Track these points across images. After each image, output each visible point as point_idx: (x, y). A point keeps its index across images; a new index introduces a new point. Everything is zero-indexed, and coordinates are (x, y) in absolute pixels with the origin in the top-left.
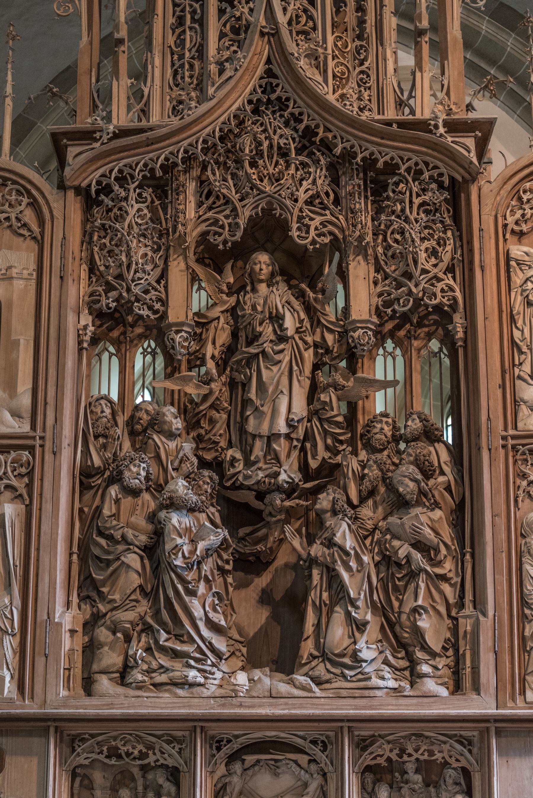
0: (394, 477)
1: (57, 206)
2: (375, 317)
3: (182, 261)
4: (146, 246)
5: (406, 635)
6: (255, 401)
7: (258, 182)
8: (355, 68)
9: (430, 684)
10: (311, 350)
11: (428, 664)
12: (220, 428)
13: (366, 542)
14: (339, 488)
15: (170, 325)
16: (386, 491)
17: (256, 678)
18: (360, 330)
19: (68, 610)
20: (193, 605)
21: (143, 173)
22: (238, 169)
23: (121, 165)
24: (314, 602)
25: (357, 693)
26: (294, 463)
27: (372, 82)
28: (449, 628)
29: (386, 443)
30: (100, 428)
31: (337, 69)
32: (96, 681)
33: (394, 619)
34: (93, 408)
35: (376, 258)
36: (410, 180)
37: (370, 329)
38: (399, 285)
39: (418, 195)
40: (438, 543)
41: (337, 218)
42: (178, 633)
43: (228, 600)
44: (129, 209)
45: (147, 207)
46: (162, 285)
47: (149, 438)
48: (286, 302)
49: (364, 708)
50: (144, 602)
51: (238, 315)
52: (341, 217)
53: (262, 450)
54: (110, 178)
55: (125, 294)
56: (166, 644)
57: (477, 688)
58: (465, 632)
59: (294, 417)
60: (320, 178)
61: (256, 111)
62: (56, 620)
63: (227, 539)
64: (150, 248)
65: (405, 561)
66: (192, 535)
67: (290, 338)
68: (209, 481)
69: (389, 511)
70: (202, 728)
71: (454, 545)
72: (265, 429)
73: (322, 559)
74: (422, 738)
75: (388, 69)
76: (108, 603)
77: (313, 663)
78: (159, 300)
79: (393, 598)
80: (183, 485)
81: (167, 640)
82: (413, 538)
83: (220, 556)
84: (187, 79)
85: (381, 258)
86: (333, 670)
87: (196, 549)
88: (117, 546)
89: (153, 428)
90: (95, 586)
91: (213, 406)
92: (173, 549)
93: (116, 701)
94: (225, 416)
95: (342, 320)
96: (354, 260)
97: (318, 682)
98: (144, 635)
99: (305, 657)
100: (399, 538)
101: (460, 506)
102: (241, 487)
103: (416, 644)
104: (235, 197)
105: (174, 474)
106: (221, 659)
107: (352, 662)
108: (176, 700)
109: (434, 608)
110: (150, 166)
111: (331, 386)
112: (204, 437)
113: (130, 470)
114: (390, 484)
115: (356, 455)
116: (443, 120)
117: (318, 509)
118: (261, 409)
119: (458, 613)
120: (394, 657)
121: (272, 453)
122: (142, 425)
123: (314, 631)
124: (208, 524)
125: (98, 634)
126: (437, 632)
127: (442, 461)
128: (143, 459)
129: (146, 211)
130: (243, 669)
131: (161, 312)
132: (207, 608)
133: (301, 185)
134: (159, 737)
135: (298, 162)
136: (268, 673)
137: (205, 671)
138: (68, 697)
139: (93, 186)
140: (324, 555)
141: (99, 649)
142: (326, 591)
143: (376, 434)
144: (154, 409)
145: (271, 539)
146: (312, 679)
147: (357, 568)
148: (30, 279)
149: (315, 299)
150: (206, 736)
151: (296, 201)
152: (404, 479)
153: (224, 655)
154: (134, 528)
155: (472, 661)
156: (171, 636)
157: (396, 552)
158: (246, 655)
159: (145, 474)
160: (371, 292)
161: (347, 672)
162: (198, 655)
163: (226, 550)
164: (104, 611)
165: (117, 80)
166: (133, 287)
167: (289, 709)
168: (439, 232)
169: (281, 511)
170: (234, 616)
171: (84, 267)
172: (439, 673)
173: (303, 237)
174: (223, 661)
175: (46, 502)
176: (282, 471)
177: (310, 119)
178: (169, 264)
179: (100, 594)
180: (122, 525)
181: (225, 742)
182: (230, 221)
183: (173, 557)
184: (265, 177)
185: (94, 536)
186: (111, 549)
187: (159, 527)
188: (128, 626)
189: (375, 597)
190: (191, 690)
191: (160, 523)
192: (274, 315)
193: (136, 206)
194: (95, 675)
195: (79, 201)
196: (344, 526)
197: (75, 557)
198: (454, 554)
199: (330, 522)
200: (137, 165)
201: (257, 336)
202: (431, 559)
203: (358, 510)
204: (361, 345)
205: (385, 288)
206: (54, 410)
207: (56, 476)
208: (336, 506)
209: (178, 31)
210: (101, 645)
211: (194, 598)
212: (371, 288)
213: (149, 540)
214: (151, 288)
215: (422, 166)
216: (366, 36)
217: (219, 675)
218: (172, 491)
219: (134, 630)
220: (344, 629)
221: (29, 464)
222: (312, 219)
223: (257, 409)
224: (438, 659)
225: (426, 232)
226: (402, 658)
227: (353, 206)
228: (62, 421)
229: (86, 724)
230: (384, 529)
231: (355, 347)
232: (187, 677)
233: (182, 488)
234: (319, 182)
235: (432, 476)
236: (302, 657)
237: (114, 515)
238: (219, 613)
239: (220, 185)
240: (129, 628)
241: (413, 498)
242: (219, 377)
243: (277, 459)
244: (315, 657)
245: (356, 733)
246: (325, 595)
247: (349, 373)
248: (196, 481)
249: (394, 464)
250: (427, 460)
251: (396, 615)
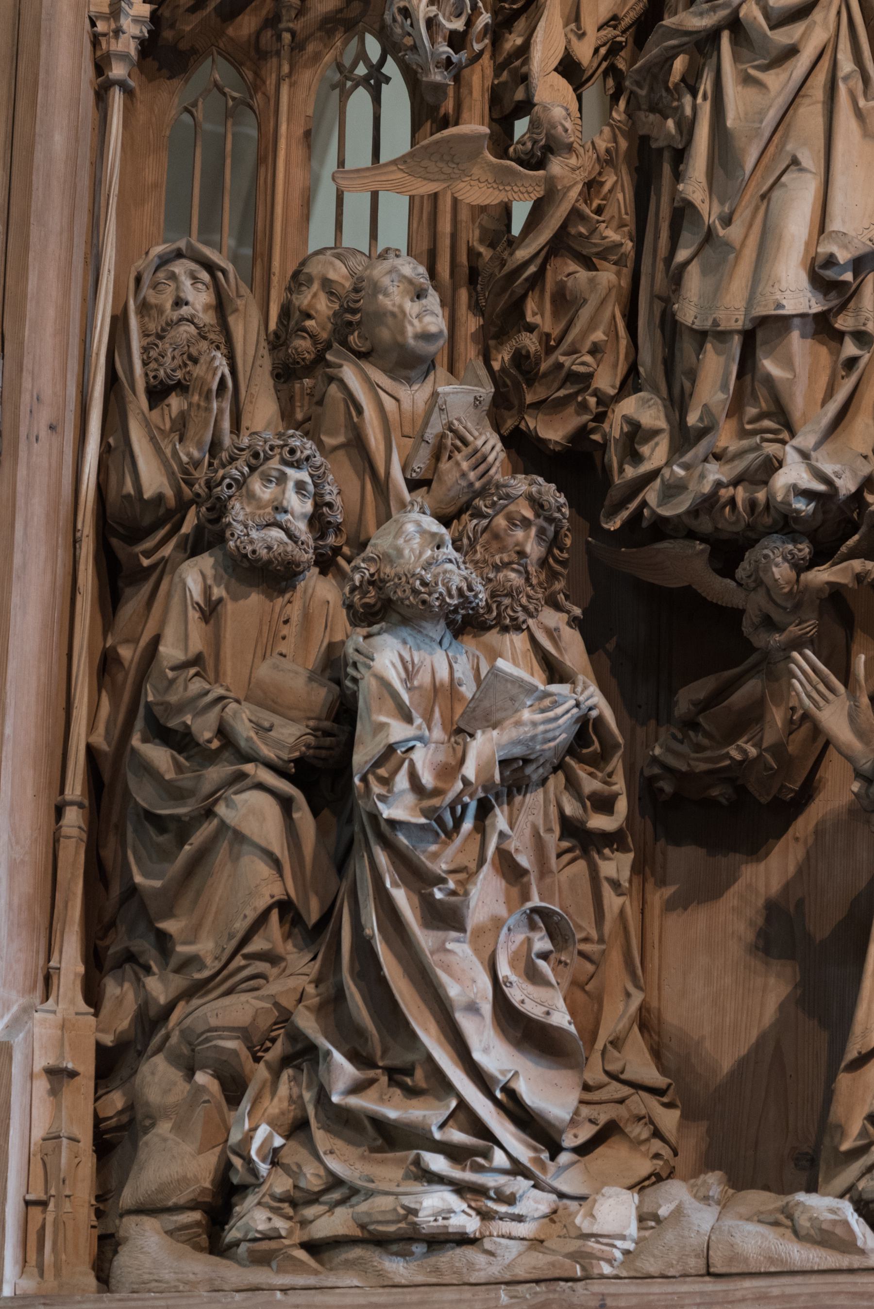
20: (451, 958)
42: (397, 1062)
56: (354, 1101)
68: (529, 514)
80: (423, 532)
81: (357, 1088)
89: (344, 343)
92: (379, 763)
98: (287, 1073)
106: (555, 1150)
113: (251, 496)
128: (292, 452)
132: (504, 970)
156: (371, 1074)
174: (564, 1158)
176: (791, 456)
211: (453, 934)
218: (385, 558)
233: (416, 541)
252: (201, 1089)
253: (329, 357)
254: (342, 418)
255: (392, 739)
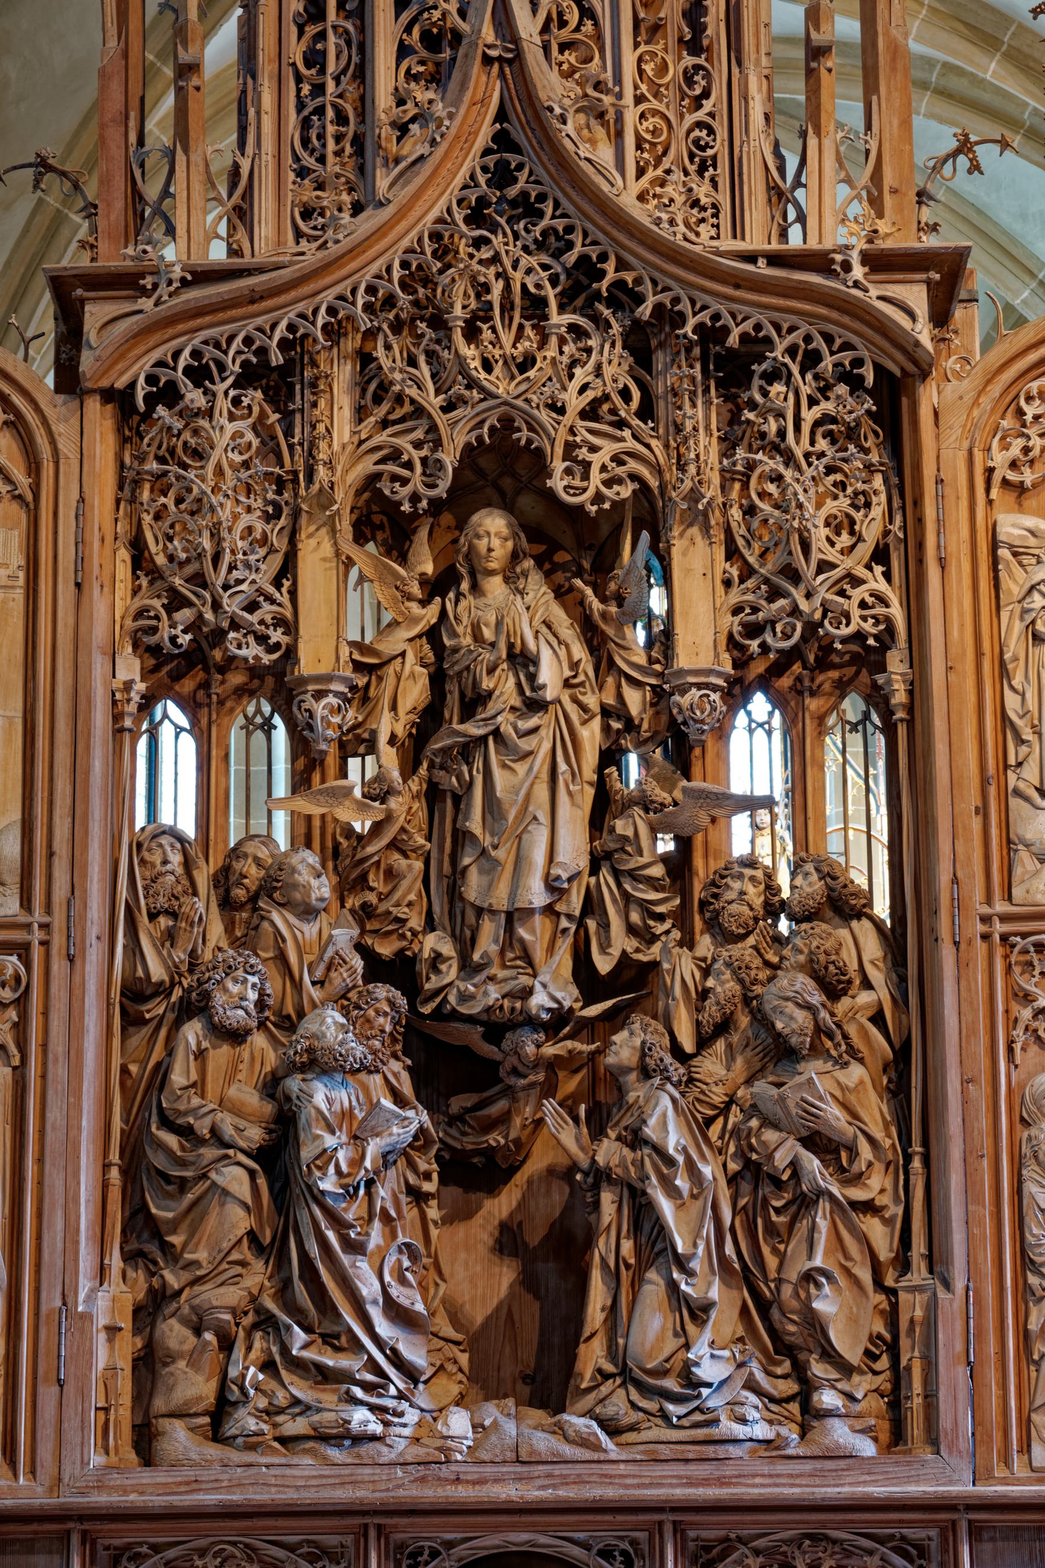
0: (766, 997)
1: (65, 431)
2: (727, 656)
3: (327, 539)
4: (249, 510)
5: (792, 1328)
6: (481, 838)
7: (483, 375)
8: (682, 116)
9: (839, 1431)
10: (597, 723)
11: (836, 1389)
12: (410, 889)
13: (710, 1134)
14: (655, 1017)
15: (304, 681)
16: (751, 1024)
17: (487, 1423)
18: (694, 690)
19: (101, 1284)
21: (243, 357)
22: (438, 342)
23: (196, 341)
24: (603, 1260)
25: (692, 1451)
26: (564, 961)
27: (719, 147)
28: (882, 1312)
29: (751, 922)
30: (161, 899)
31: (645, 124)
32: (163, 1433)
33: (768, 1293)
34: (146, 854)
35: (728, 531)
36: (795, 370)
37: (715, 688)
38: (774, 594)
39: (812, 402)
40: (856, 1137)
41: (648, 446)
42: (328, 1331)
43: (429, 1256)
44: (216, 435)
45: (254, 428)
46: (284, 590)
47: (263, 918)
48: (544, 622)
49: (706, 1482)
50: (258, 1265)
51: (444, 646)
52: (654, 443)
53: (496, 941)
54: (175, 369)
55: (209, 616)
56: (306, 1354)
57: (933, 1442)
58: (912, 1321)
59: (560, 872)
60: (610, 362)
61: (477, 216)
62: (80, 1309)
63: (427, 1129)
64: (259, 513)
65: (788, 1172)
66: (355, 1125)
67: (552, 703)
68: (388, 1010)
69: (758, 1066)
70: (379, 1528)
71: (889, 1136)
72: (500, 898)
73: (619, 1171)
74: (824, 1544)
75: (751, 119)
76: (183, 1268)
77: (602, 1388)
78: (280, 622)
79: (766, 1250)
80: (335, 1023)
81: (305, 1346)
82: (804, 1126)
83: (412, 1165)
84: (331, 146)
85: (739, 531)
86: (643, 1404)
87: (363, 1157)
88: (202, 1151)
89: (270, 897)
90: (155, 1230)
91: (394, 845)
92: (316, 1158)
93: (205, 1475)
94: (418, 865)
95: (658, 662)
96: (681, 535)
97: (612, 1429)
98: (258, 1335)
99: (588, 1375)
100: (776, 1126)
101: (902, 1054)
102: (455, 1015)
103: (811, 1346)
104: (433, 402)
105: (316, 993)
106: (416, 1382)
107: (682, 1386)
108: (327, 1471)
109: (847, 1271)
110: (258, 343)
111: (636, 804)
112: (377, 907)
113: (226, 990)
114: (759, 1011)
115: (691, 946)
116: (861, 251)
117: (612, 1065)
118: (493, 853)
119: (897, 1281)
120: (768, 1373)
121: (517, 945)
122: (247, 889)
123: (606, 1320)
124: (387, 1103)
125: (163, 1332)
126: (853, 1320)
127: (865, 959)
128: (252, 966)
129: (250, 436)
130: (460, 1401)
131: (284, 648)
132: (387, 1278)
133: (571, 376)
134: (291, 1548)
135: (564, 329)
136: (513, 1411)
137: (384, 1410)
138: (106, 1467)
139: (139, 388)
140: (623, 1163)
141: (166, 1364)
142: (628, 1238)
143: (730, 903)
144: (272, 856)
145: (518, 1121)
146: (602, 1423)
147: (691, 1190)
148: (13, 587)
149: (604, 615)
150: (387, 1544)
151: (561, 411)
152: (785, 1004)
153: (422, 1373)
154: (237, 1111)
155: (926, 1382)
156: (314, 1336)
157: (770, 1157)
158: (466, 1370)
159: (256, 996)
160: (718, 606)
161: (671, 1407)
162: (370, 1377)
163: (423, 1149)
164: (176, 1286)
165: (186, 150)
166: (225, 601)
167: (554, 1487)
168: (858, 480)
169: (536, 1066)
170: (443, 1287)
171: (124, 554)
172: (858, 1408)
173: (576, 488)
174: (421, 1386)
175: (56, 1060)
176: (538, 987)
177: (588, 241)
178: (300, 546)
179: (166, 1248)
180: (212, 1106)
181: (425, 1557)
182: (424, 452)
183: (317, 1174)
184: (497, 361)
185: (154, 1129)
186: (190, 1156)
187: (286, 1108)
188: (227, 1317)
189: (729, 1249)
190: (356, 1450)
191: (288, 1099)
192: (518, 650)
193: (230, 428)
194: (160, 1420)
195: (109, 415)
196: (666, 1102)
197: (114, 1173)
198: (890, 1157)
199: (636, 1092)
200: (230, 339)
201: (483, 698)
202: (843, 1170)
203: (695, 1062)
204: (696, 721)
205: (745, 598)
206: (68, 867)
207: (76, 1005)
208: (647, 1059)
209: (311, 30)
210: (171, 1358)
211: (360, 1257)
212: (718, 594)
213: (267, 1137)
214: (261, 599)
215: (819, 343)
216: (705, 42)
217: (412, 1416)
218: (314, 1036)
219: (237, 1325)
220: (665, 1318)
221: (17, 979)
222: (594, 449)
223: (484, 852)
224: (856, 1378)
225: (832, 478)
226: (785, 1377)
227: (679, 421)
228: (85, 891)
229: (144, 1525)
230: (748, 1104)
231: (685, 723)
232: (349, 1422)
234: (608, 371)
235: (844, 992)
236: (581, 1376)
237: (194, 1085)
238: (410, 1286)
239: (403, 380)
240: (229, 1322)
241: (802, 1043)
242: (405, 781)
243: (527, 958)
244: (606, 1376)
245: (692, 1534)
246: (627, 1246)
247: (674, 773)
248: (361, 1009)
249: (767, 964)
250: (833, 962)
251: (772, 1285)
252: (207, 1343)
253: (261, 904)
254: (271, 942)
255: (327, 1146)
